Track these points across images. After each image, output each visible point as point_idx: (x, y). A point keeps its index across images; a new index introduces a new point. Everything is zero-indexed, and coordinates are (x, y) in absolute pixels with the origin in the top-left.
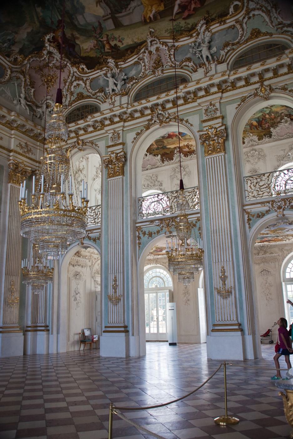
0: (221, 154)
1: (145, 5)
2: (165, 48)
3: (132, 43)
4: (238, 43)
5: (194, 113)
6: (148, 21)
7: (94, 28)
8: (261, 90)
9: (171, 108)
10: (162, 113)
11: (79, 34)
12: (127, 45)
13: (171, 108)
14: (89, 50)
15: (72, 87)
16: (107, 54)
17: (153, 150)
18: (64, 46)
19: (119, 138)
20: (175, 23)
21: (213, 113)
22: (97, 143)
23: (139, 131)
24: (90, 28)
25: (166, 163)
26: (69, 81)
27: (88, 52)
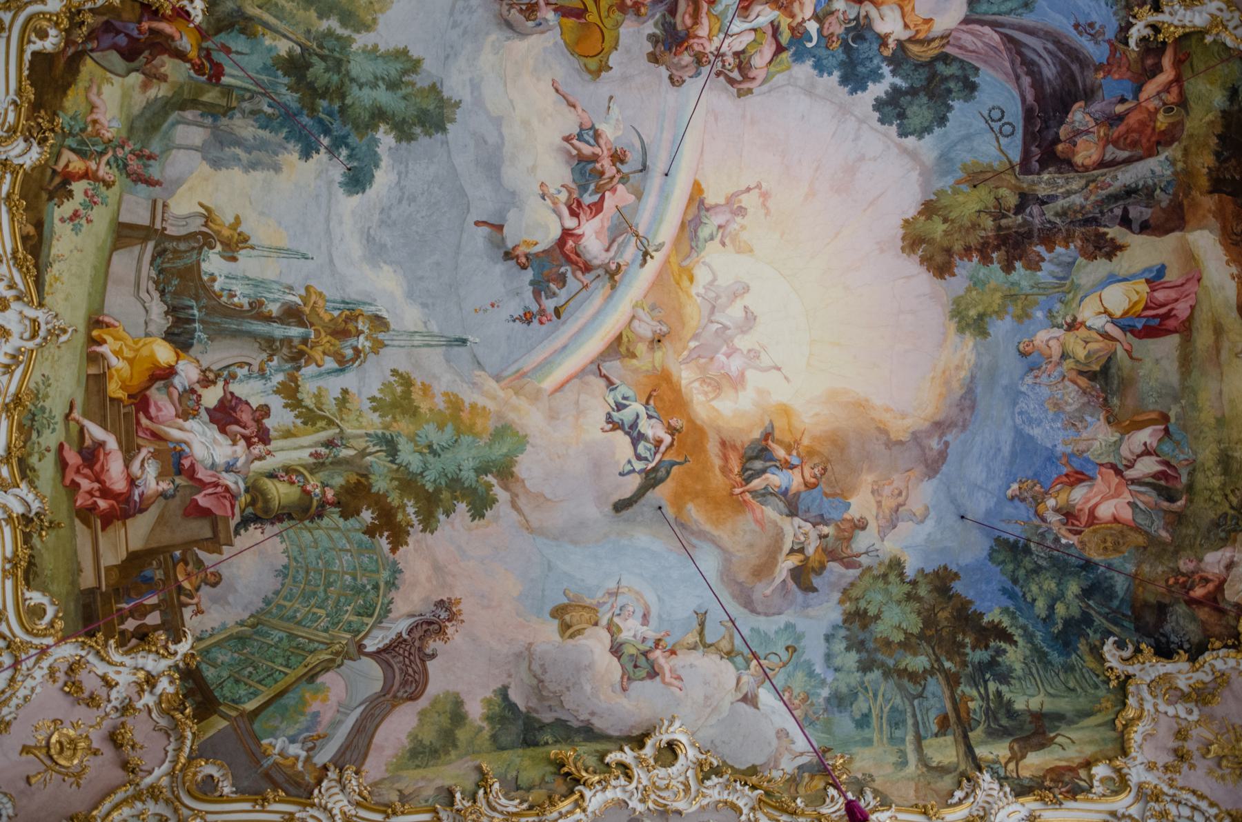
1: (141, 344)
3: (54, 251)
6: (95, 333)
7: (150, 157)
11: (156, 99)
12: (52, 232)
14: (94, 98)
16: (55, 150)
18: (145, 25)
20: (59, 418)
24: (155, 146)
27: (88, 89)
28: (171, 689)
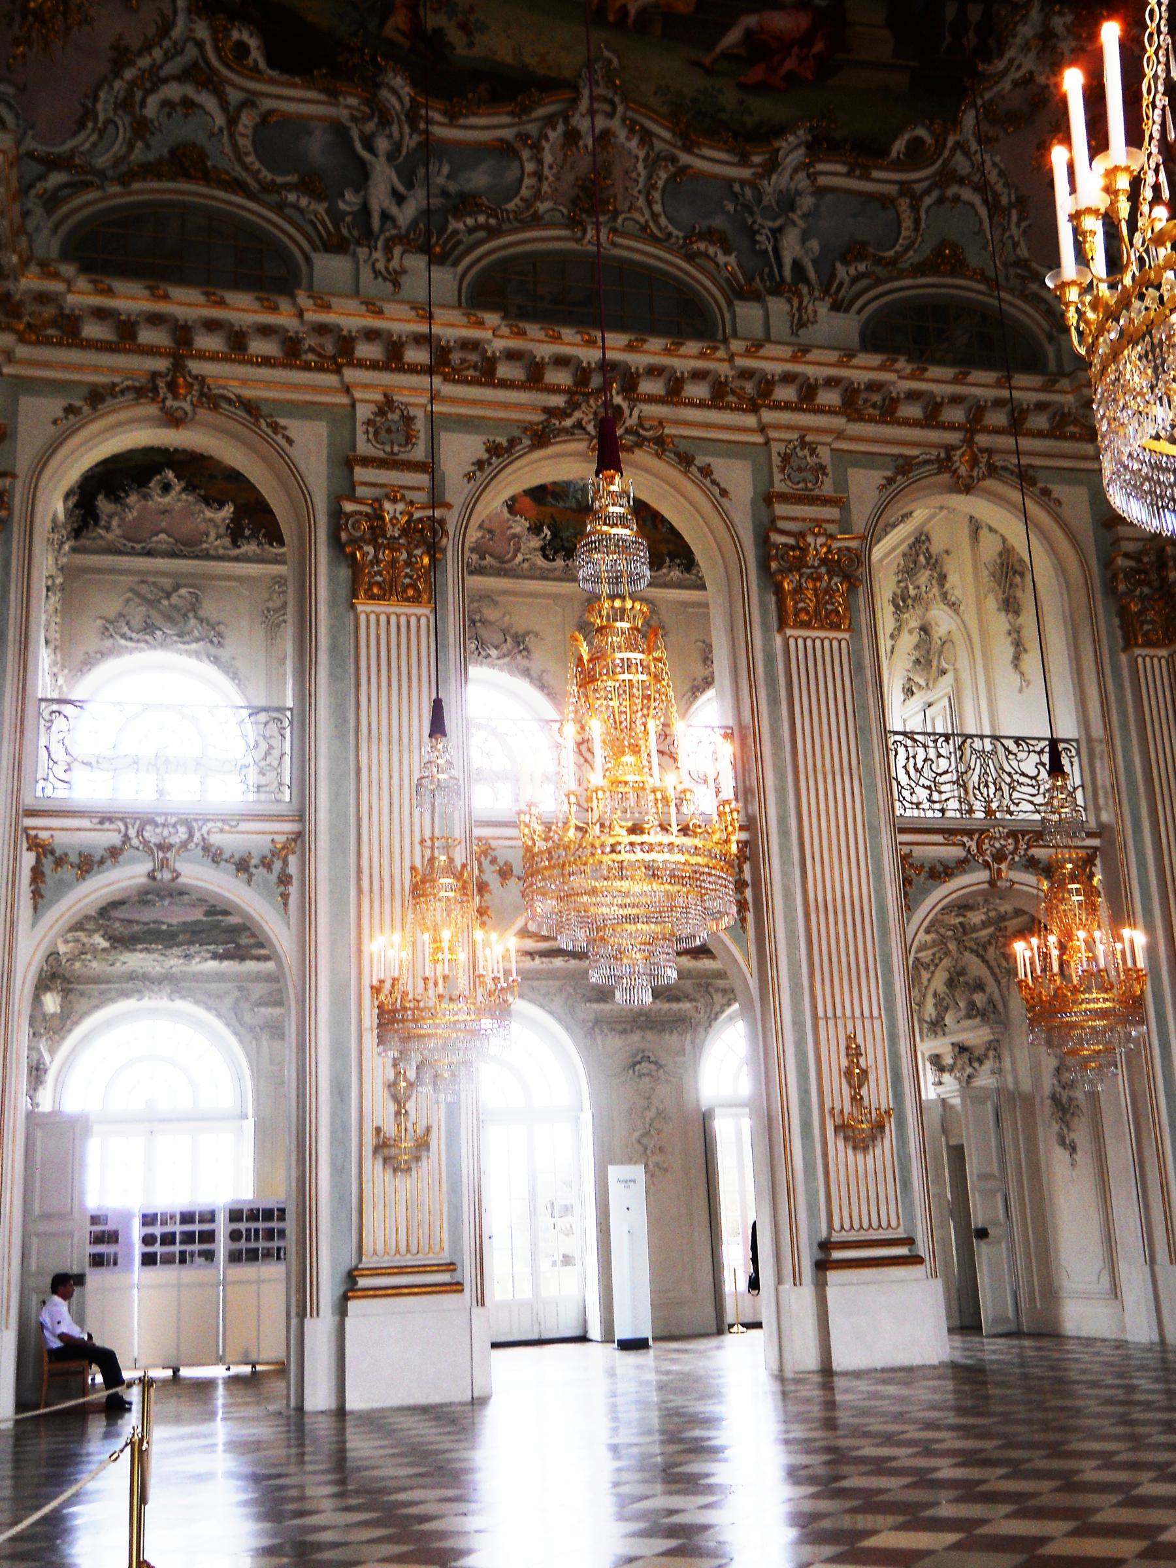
0: (840, 635)
2: (636, 151)
3: (509, 59)
4: (894, 262)
5: (734, 450)
6: (611, 18)
8: (963, 455)
9: (651, 399)
10: (625, 405)
13: (651, 399)
15: (153, 101)
17: (212, 477)
19: (409, 439)
21: (810, 476)
22: (282, 422)
23: (505, 444)
25: (250, 548)
26: (144, 62)
28: (1069, 18)
